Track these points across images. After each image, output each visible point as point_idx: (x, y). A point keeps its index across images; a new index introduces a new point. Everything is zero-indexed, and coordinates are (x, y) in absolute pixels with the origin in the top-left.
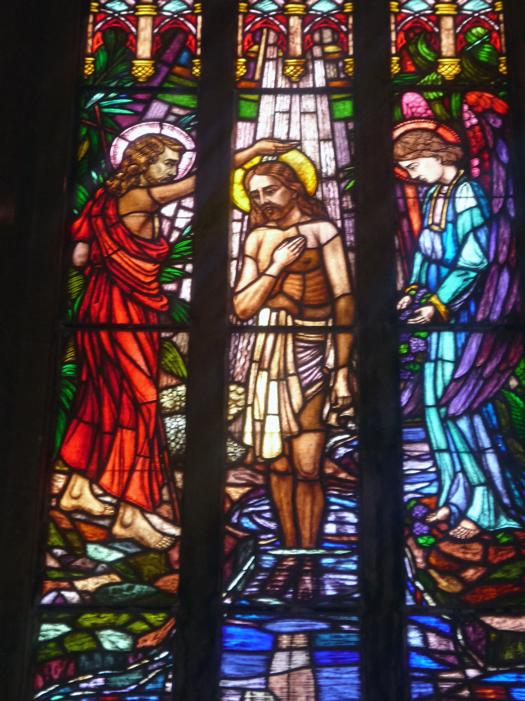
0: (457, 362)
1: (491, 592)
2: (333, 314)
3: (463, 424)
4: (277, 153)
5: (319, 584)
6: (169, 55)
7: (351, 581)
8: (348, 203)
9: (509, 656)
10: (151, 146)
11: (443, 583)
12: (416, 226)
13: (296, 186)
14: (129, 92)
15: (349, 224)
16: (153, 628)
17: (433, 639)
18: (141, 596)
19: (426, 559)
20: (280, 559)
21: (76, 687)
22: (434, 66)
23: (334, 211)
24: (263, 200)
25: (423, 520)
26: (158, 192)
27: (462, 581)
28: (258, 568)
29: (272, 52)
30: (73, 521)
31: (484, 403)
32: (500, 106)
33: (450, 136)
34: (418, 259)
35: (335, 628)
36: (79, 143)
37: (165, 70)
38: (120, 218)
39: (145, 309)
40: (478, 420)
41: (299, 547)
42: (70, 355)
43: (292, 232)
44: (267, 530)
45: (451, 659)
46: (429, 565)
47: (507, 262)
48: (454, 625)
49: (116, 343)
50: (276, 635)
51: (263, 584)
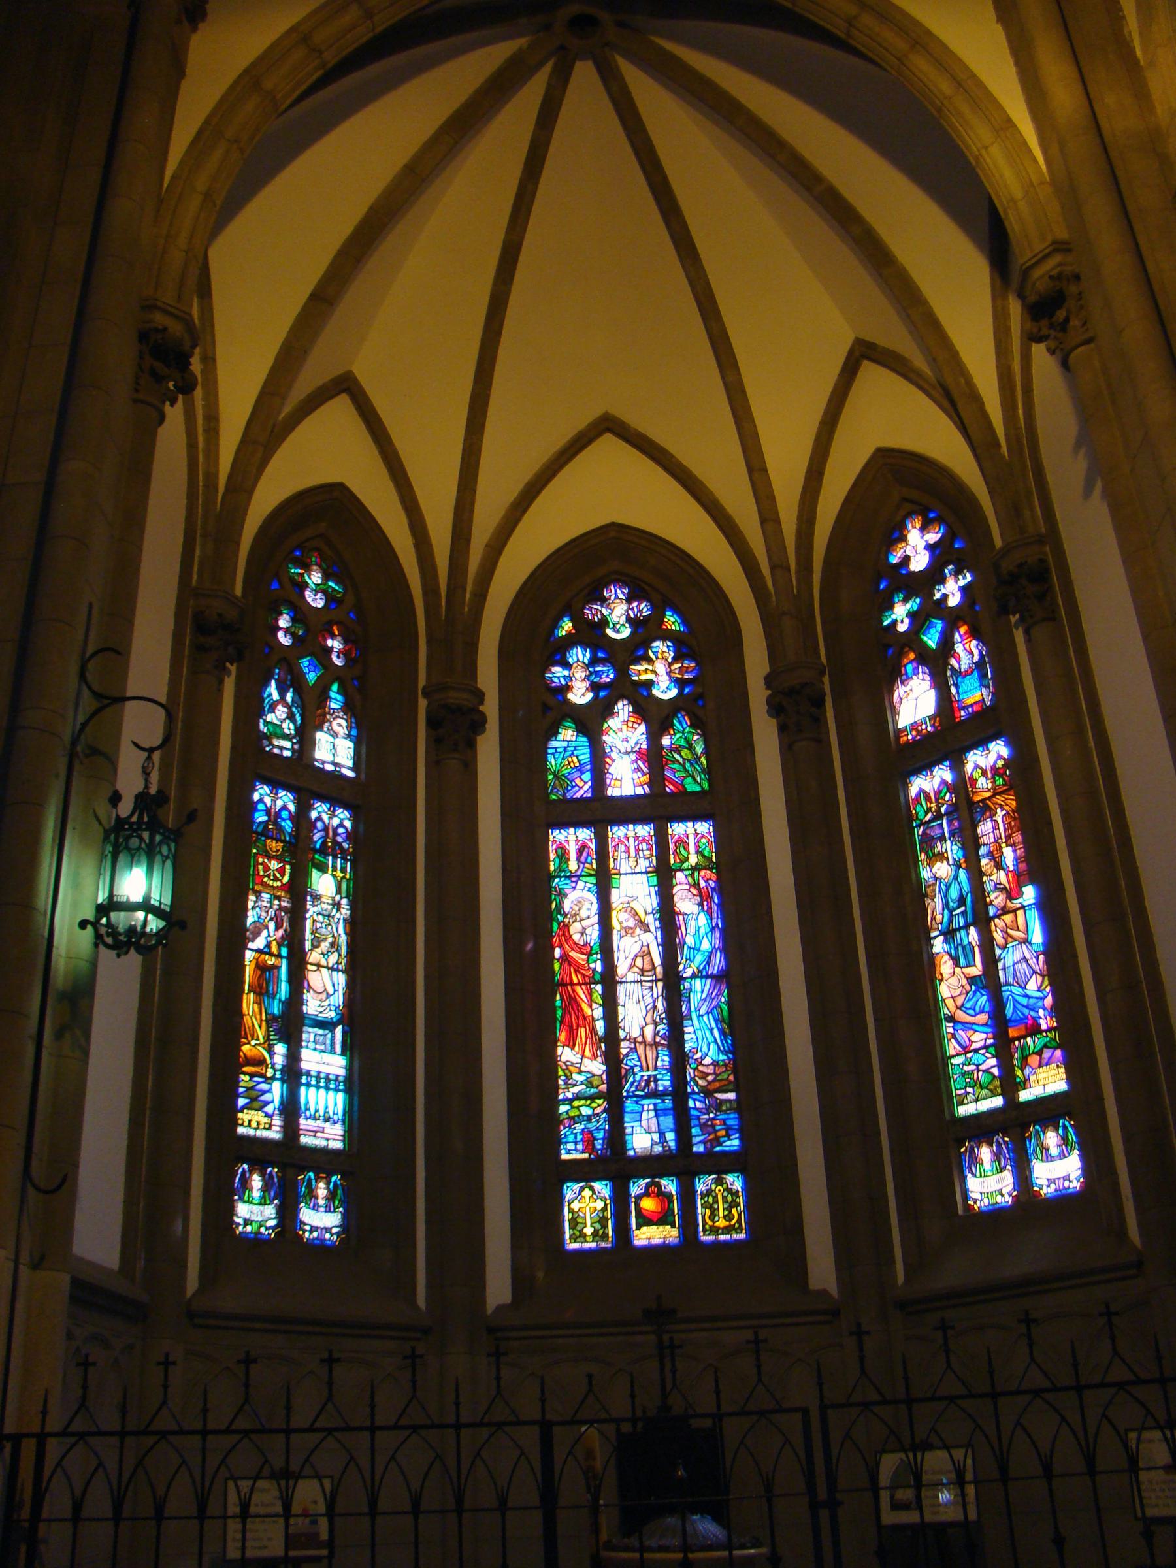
0: (702, 992)
1: (717, 1085)
2: (655, 974)
3: (705, 1018)
4: (628, 903)
5: (656, 1085)
6: (583, 859)
7: (668, 1083)
8: (658, 924)
9: (724, 1108)
10: (580, 902)
11: (700, 1082)
12: (684, 934)
13: (637, 918)
14: (570, 877)
15: (659, 934)
16: (599, 1106)
17: (698, 1103)
18: (594, 1094)
19: (694, 1073)
20: (642, 1076)
21: (574, 1129)
22: (687, 859)
23: (652, 928)
24: (625, 925)
25: (692, 1058)
26: (585, 923)
27: (707, 1081)
28: (635, 1081)
29: (624, 855)
30: (566, 1065)
31: (713, 1009)
32: (714, 877)
33: (695, 892)
34: (686, 947)
35: (663, 1101)
36: (551, 903)
37: (582, 866)
38: (571, 936)
39: (584, 976)
40: (710, 1015)
41: (648, 1070)
42: (558, 997)
43: (637, 939)
44: (637, 1066)
45: (703, 1111)
46: (695, 1076)
47: (719, 947)
48: (704, 1097)
49: (574, 991)
50: (643, 1105)
51: (637, 1087)
